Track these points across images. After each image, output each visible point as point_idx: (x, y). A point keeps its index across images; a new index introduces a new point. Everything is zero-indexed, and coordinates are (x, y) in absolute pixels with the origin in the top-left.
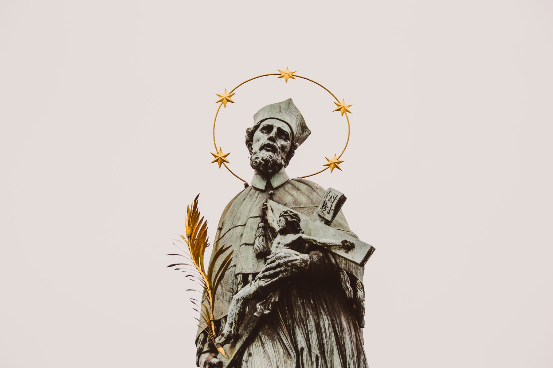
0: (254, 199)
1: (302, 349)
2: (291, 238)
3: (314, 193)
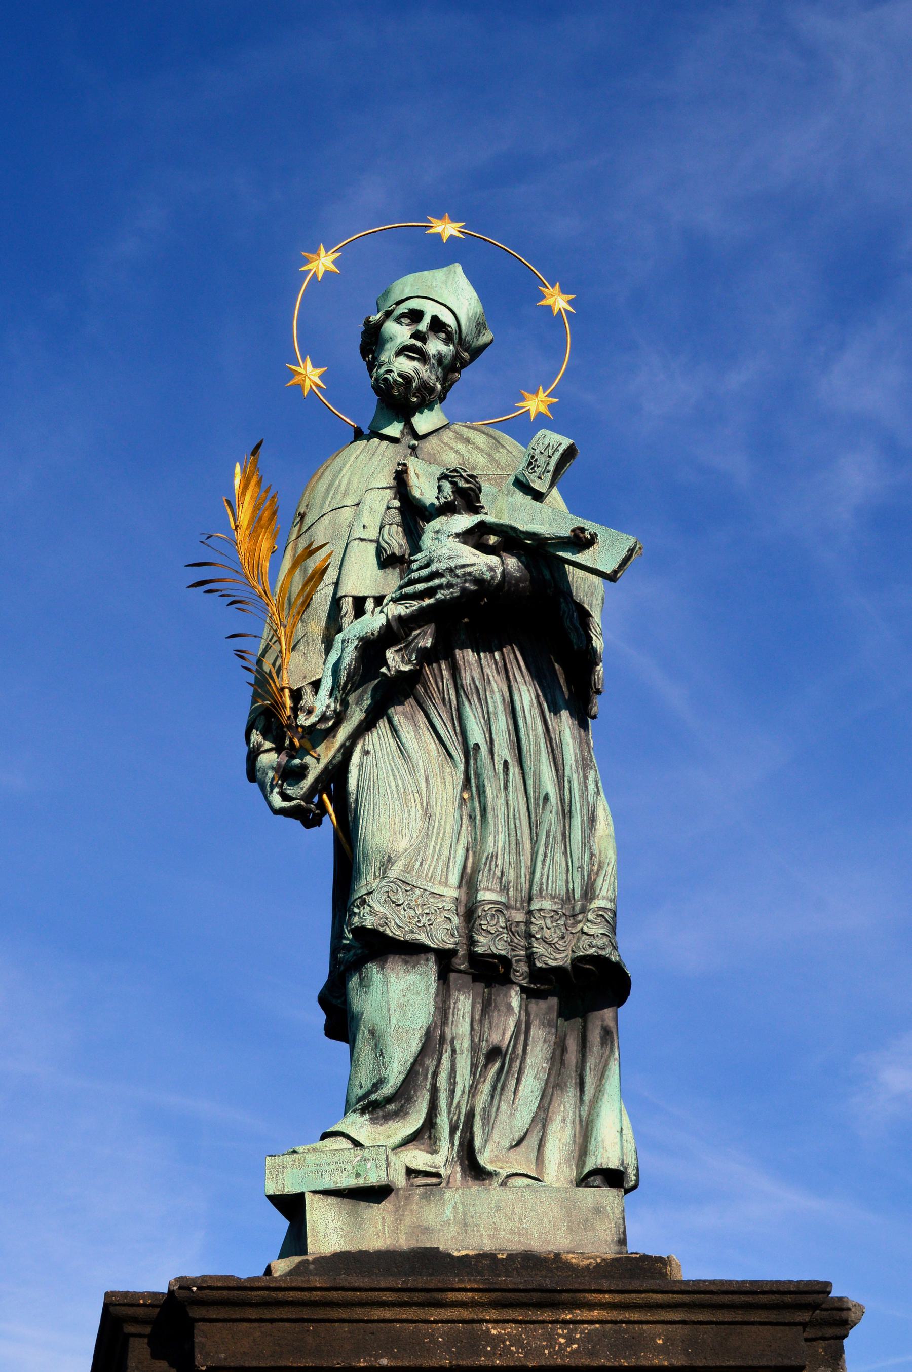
0: (377, 457)
2: (464, 521)
3: (501, 450)
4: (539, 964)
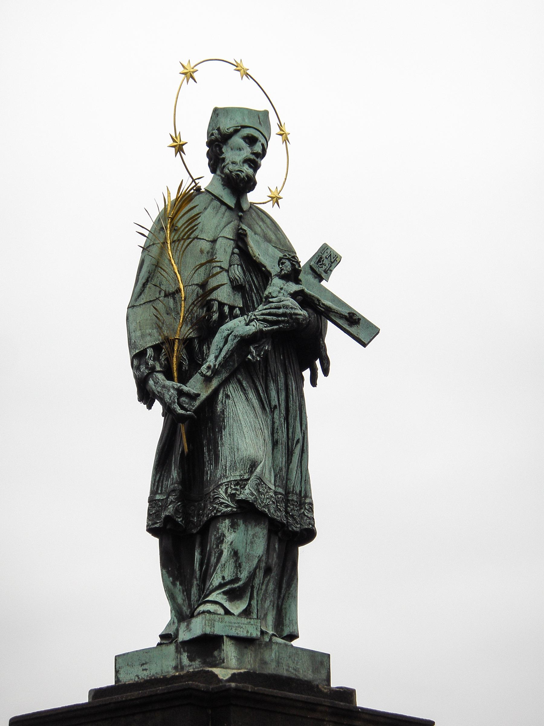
0: (220, 215)
1: (275, 407)
2: (293, 287)
4: (290, 529)
